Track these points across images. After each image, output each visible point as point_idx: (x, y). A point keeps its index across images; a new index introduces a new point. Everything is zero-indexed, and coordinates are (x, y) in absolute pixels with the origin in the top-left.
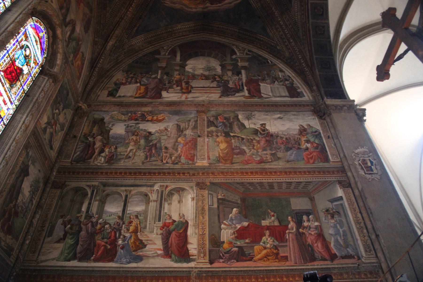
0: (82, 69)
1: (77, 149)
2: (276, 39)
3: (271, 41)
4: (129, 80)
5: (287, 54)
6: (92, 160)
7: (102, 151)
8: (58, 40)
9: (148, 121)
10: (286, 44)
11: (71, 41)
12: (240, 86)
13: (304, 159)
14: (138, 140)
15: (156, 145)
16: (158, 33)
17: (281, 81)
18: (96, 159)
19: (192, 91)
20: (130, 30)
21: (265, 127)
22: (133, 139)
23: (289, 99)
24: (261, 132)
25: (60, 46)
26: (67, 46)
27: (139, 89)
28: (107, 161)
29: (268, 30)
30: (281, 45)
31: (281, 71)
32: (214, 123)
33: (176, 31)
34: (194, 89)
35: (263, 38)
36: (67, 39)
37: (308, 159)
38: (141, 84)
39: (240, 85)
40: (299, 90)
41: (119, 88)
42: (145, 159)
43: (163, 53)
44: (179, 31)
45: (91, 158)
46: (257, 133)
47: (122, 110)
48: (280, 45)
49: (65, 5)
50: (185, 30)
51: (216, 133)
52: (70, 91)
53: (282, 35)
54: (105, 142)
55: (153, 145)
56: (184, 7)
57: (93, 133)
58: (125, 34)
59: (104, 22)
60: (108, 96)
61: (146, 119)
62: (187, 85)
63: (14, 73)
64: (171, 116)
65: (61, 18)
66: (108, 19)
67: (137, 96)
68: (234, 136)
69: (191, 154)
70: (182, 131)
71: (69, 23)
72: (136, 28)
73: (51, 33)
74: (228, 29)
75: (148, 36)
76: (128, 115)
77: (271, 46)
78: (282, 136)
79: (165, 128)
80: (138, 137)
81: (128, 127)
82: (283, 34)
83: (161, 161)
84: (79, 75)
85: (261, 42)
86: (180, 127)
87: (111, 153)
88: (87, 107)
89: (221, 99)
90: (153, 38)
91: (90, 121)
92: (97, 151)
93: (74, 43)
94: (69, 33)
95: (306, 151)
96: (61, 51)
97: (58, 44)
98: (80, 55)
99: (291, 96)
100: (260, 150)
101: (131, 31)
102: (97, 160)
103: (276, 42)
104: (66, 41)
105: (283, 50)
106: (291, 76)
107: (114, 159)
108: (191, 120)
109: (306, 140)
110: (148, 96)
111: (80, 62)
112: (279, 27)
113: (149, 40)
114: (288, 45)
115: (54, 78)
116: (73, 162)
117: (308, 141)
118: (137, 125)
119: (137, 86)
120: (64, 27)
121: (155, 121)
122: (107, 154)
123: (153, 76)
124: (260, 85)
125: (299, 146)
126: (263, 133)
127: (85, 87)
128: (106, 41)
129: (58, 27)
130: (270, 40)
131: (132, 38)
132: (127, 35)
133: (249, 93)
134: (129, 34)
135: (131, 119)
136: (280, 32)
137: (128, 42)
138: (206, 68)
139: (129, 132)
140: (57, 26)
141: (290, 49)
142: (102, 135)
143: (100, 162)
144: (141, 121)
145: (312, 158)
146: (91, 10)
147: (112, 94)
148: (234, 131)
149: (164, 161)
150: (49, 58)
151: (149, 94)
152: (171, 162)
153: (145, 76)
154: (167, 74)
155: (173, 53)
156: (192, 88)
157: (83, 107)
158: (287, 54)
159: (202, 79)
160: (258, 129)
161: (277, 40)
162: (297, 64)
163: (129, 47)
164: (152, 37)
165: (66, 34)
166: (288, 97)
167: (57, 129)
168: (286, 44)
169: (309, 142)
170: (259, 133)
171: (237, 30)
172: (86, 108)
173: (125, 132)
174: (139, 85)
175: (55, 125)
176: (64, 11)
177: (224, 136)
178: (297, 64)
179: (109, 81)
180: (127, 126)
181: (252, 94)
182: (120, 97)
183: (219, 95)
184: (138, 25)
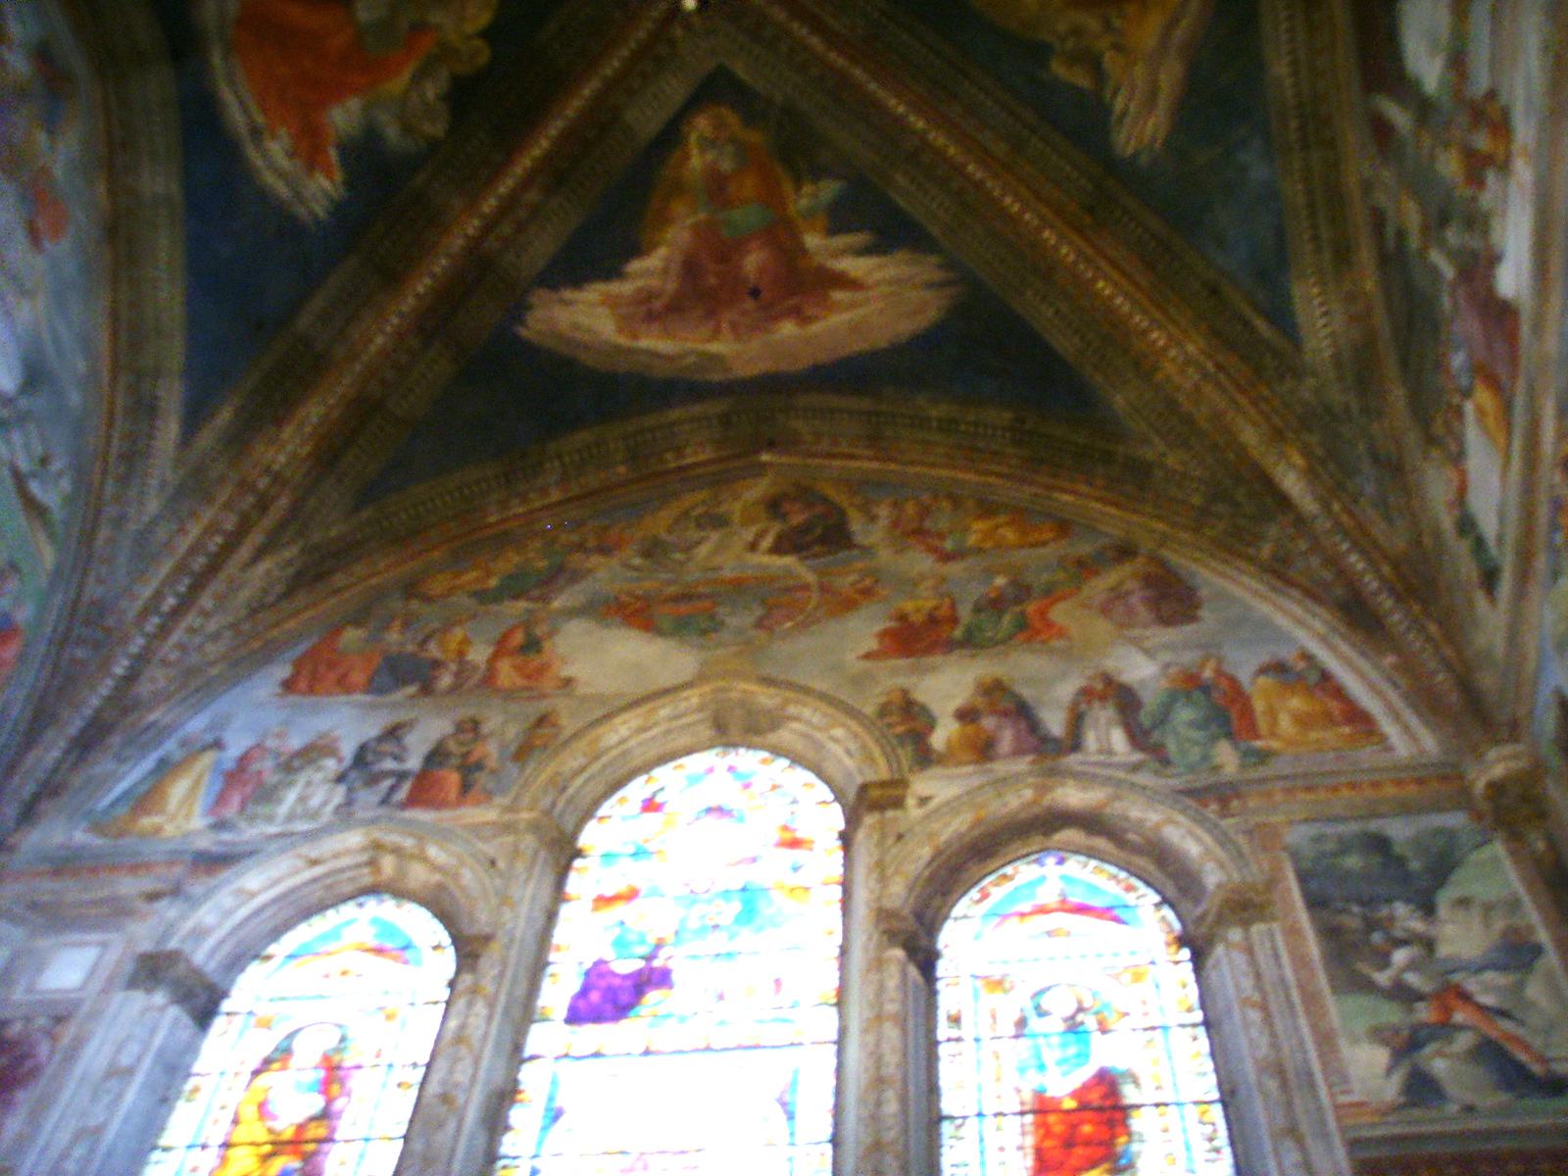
0: (1339, 693)
4: (1453, 448)
8: (1108, 810)
11: (1156, 736)
25: (1135, 813)
26: (1165, 761)
36: (1137, 757)
43: (1381, 199)
47: (1541, 563)
49: (988, 723)
52: (1373, 826)
56: (1179, 34)
63: (1082, 1122)
65: (1022, 765)
71: (1077, 722)
73: (1070, 835)
84: (1347, 730)
88: (1508, 749)
93: (1184, 714)
94: (1118, 739)
96: (1153, 817)
97: (1127, 819)
98: (1260, 692)
104: (1136, 768)
111: (1296, 703)
115: (1244, 907)
120: (1072, 760)
127: (1426, 701)
128: (1284, 501)
129: (1049, 797)
140: (1047, 800)
146: (1124, 552)
150: (1171, 892)
151: (1502, 372)
154: (1444, 221)
155: (1381, 131)
156: (1492, 95)
157: (1498, 771)
164: (1315, 238)
165: (1110, 752)
167: (1487, 1000)
172: (1515, 757)
175: (1454, 1002)
176: (1007, 739)
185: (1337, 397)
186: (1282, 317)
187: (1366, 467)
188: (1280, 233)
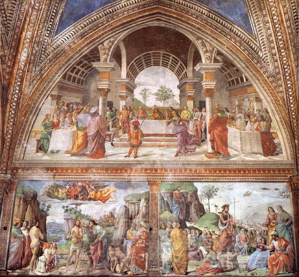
1: (11, 250)
2: (260, 39)
3: (252, 39)
5: (271, 68)
6: (29, 267)
7: (40, 253)
9: (90, 199)
10: (274, 51)
12: (202, 132)
13: (267, 267)
14: (81, 233)
15: (101, 241)
16: (93, 19)
17: (256, 121)
18: (35, 265)
19: (143, 143)
20: (50, 21)
21: (227, 212)
22: (74, 232)
23: (262, 158)
24: (222, 220)
27: (74, 136)
28: (48, 269)
29: (251, 20)
30: (265, 51)
31: (258, 100)
32: (168, 204)
33: (119, 11)
34: (145, 138)
35: (241, 31)
37: (273, 266)
38: (77, 126)
39: (203, 130)
40: (276, 141)
41: (50, 134)
42: (90, 267)
43: (103, 57)
44: (123, 9)
45: (27, 264)
46: (218, 222)
48: (263, 50)
50: (132, 6)
51: (170, 222)
53: (270, 35)
54: (42, 238)
55: (98, 242)
57: (25, 220)
58: (44, 29)
59: (5, 19)
60: (37, 152)
61: (89, 197)
62: (136, 131)
64: (117, 190)
66: (9, 12)
67: (75, 150)
68: (191, 228)
69: (142, 257)
70: (131, 219)
72: (58, 17)
74: (192, 8)
75: (79, 27)
76: (66, 188)
77: (251, 47)
78: (246, 227)
79: (111, 213)
80: (80, 229)
81: (67, 211)
82: (273, 35)
83: (108, 269)
85: (238, 39)
86: (129, 211)
87: (51, 255)
89: (177, 158)
90: (86, 28)
91: (20, 199)
92: (34, 252)
95: (272, 253)
99: (266, 154)
100: (219, 253)
101: (51, 23)
102: (36, 268)
103: (260, 44)
105: (267, 59)
106: (269, 110)
107: (55, 265)
108: (141, 200)
109: (275, 235)
110: (88, 152)
112: (270, 21)
113: (82, 31)
114: (275, 54)
116: (8, 271)
117: (276, 237)
118: (78, 207)
119: (74, 132)
121: (99, 200)
122: (47, 257)
123: (93, 110)
124: (227, 130)
125: (264, 245)
126: (224, 222)
130: (250, 38)
131: (56, 34)
132: (48, 30)
133: (213, 148)
134: (49, 29)
135: (69, 196)
136: (269, 29)
137: (51, 42)
138: (160, 93)
139: (69, 219)
141: (277, 61)
142: (37, 225)
143: (40, 270)
144: (82, 200)
145: (277, 264)
147: (41, 148)
148: (191, 219)
149: (111, 269)
152: (119, 272)
153: (82, 109)
158: (271, 68)
159: (156, 119)
160: (218, 214)
161: (261, 42)
162: (281, 89)
163: (55, 49)
166: (261, 154)
168: (274, 51)
169: (277, 239)
170: (220, 223)
171: (206, 12)
173: (64, 219)
174: (75, 128)
177: (180, 228)
178: (281, 89)
179: (36, 119)
180: (65, 208)
181: (216, 150)
182: (52, 152)
183: (175, 150)
184: (60, 12)
185: (50, 49)
186: (63, 25)
187: (38, 69)
188: (83, 15)
